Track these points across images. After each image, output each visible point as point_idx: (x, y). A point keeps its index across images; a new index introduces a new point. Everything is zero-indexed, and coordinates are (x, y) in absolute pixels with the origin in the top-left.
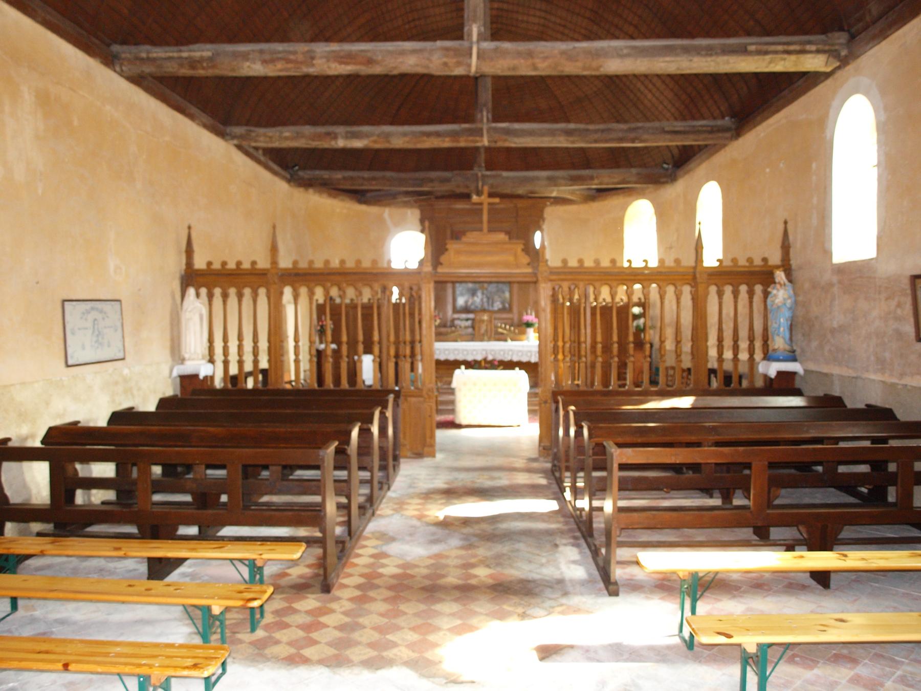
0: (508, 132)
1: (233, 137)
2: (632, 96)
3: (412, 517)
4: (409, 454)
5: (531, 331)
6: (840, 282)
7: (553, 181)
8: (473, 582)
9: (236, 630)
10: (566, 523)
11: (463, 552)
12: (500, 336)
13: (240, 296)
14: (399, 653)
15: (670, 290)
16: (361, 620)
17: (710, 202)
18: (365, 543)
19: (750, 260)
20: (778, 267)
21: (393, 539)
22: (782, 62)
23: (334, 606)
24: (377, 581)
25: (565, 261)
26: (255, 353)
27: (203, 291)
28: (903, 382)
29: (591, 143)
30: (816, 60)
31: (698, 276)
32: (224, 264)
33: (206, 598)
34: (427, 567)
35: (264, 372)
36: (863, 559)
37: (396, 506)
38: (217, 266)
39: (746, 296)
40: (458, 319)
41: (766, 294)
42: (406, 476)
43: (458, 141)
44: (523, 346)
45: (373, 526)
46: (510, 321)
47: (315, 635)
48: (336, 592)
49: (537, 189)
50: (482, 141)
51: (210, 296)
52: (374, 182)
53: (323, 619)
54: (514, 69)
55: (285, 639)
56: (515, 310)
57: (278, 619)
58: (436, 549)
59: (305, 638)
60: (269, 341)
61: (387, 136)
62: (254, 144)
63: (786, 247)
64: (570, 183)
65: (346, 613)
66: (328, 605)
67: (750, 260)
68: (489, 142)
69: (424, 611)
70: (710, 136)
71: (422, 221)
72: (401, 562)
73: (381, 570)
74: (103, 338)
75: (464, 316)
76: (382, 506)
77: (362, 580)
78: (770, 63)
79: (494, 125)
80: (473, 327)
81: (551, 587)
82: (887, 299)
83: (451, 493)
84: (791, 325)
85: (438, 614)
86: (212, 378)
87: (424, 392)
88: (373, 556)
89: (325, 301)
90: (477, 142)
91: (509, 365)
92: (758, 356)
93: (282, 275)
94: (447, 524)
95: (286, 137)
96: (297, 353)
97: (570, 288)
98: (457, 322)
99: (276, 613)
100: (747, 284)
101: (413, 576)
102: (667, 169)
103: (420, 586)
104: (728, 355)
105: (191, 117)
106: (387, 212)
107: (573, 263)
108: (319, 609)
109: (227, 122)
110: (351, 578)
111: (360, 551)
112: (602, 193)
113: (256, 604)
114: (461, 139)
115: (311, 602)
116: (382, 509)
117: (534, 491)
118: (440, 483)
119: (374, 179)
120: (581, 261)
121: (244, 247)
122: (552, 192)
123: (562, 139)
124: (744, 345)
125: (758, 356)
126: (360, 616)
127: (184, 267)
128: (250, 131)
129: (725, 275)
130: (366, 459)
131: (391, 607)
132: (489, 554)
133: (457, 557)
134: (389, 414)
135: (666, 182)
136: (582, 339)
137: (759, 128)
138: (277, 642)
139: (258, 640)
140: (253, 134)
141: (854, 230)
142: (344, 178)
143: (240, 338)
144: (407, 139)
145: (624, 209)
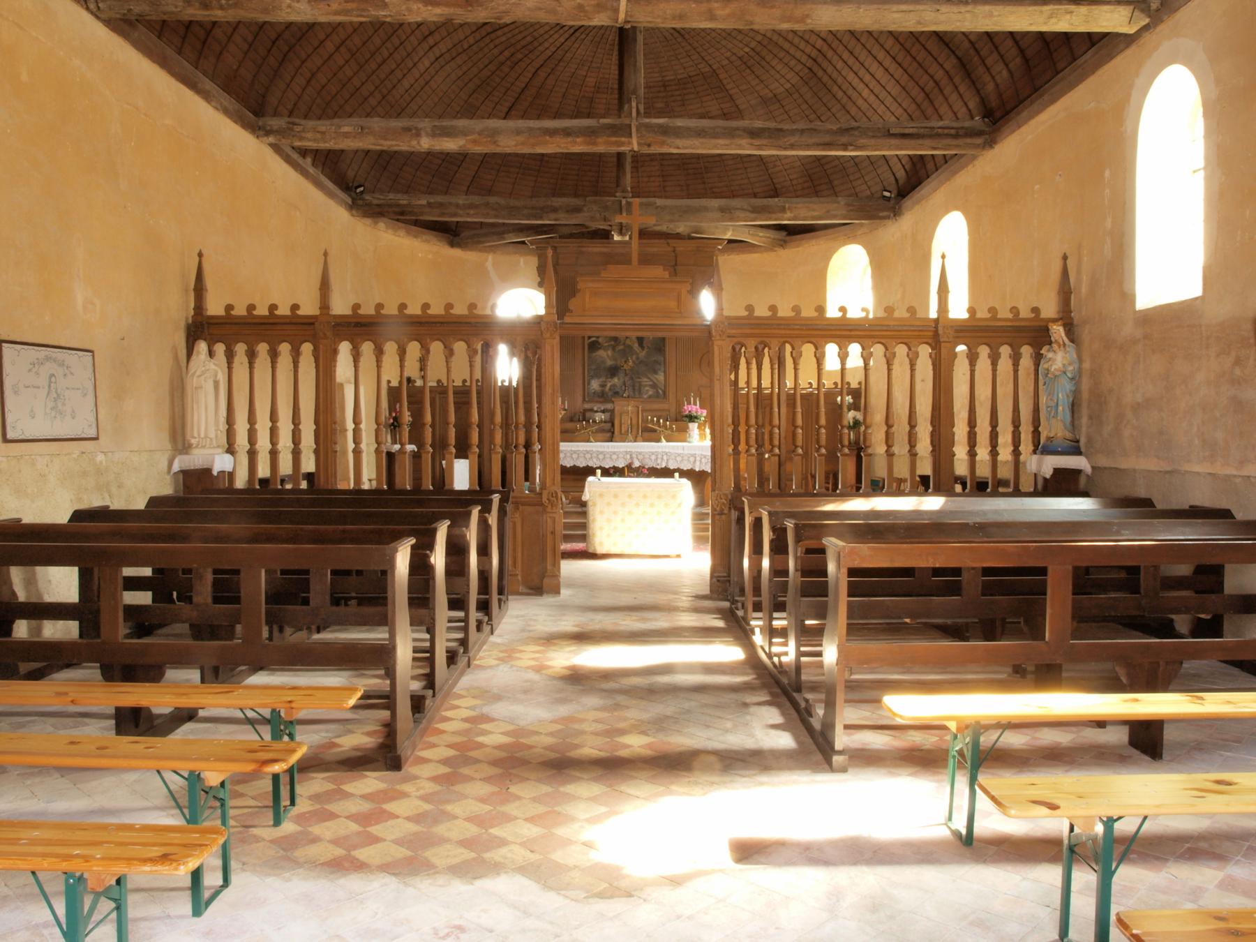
0: (665, 131)
1: (268, 133)
2: (840, 94)
3: (528, 668)
4: (521, 589)
5: (694, 427)
6: (1146, 337)
7: (727, 213)
8: (623, 753)
9: (248, 823)
10: (759, 677)
11: (605, 715)
12: (653, 435)
13: (274, 355)
14: (509, 855)
15: (901, 350)
16: (449, 808)
17: (951, 238)
18: (456, 702)
19: (1014, 310)
20: (1054, 321)
21: (498, 698)
22: (1068, 17)
23: (407, 788)
24: (472, 754)
25: (750, 308)
26: (296, 453)
27: (220, 348)
28: (1245, 473)
29: (785, 149)
30: (1116, 15)
31: (940, 332)
32: (251, 307)
33: (196, 759)
34: (551, 734)
35: (309, 477)
36: (1229, 702)
37: (501, 655)
38: (240, 311)
39: (1010, 362)
41: (1038, 358)
42: (517, 617)
43: (595, 144)
45: (467, 680)
47: (375, 830)
48: (409, 769)
49: (704, 225)
50: (630, 143)
51: (230, 356)
52: (472, 212)
53: (389, 807)
54: (681, 17)
55: (328, 835)
57: (318, 806)
58: (563, 710)
59: (359, 833)
60: (316, 422)
61: (494, 133)
62: (297, 144)
63: (1065, 292)
64: (753, 215)
65: (424, 798)
66: (398, 787)
67: (1014, 310)
68: (639, 144)
69: (547, 794)
70: (954, 142)
71: (541, 270)
72: (511, 728)
73: (480, 739)
74: (64, 404)
76: (481, 654)
77: (451, 753)
78: (1050, 17)
79: (647, 120)
81: (743, 761)
82: (1218, 356)
83: (582, 638)
84: (1073, 405)
85: (572, 798)
86: (231, 475)
87: (545, 499)
88: (466, 720)
89: (400, 382)
90: (623, 144)
91: (666, 473)
92: (1026, 447)
93: (337, 325)
94: (578, 679)
95: (346, 136)
96: (357, 440)
97: (756, 348)
98: (588, 415)
99: (315, 798)
100: (1011, 345)
101: (531, 747)
102: (888, 199)
103: (541, 759)
104: (983, 453)
105: (206, 96)
106: (490, 260)
107: (761, 311)
108: (384, 792)
109: (259, 112)
110: (435, 750)
111: (449, 714)
112: (794, 232)
113: (277, 768)
114: (600, 140)
115: (372, 782)
116: (481, 658)
117: (706, 633)
118: (569, 624)
119: (471, 206)
120: (773, 308)
121: (285, 288)
122: (726, 229)
123: (744, 142)
124: (1005, 439)
125: (1026, 447)
126: (448, 802)
127: (192, 313)
128: (294, 124)
129: (978, 332)
130: (458, 581)
131: (496, 789)
132: (645, 716)
133: (595, 721)
134: (493, 520)
135: (888, 218)
136: (776, 422)
137: (1024, 129)
138: (315, 840)
139: (285, 837)
140: (297, 129)
141: (1168, 262)
142: (430, 205)
143: (274, 417)
144: (520, 138)
145: (827, 259)
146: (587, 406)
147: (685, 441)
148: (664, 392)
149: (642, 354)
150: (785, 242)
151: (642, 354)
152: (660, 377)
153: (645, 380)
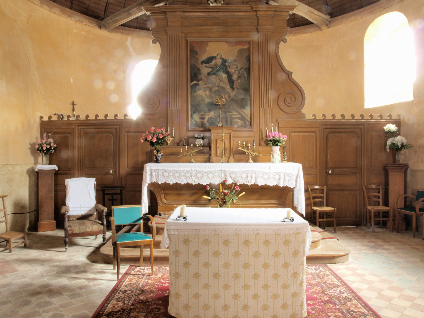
5: (277, 150)
12: (242, 156)
98: (191, 140)
146: (190, 134)
147: (269, 161)
150: (330, 22)
151: (233, 94)
152: (247, 111)
153: (235, 114)
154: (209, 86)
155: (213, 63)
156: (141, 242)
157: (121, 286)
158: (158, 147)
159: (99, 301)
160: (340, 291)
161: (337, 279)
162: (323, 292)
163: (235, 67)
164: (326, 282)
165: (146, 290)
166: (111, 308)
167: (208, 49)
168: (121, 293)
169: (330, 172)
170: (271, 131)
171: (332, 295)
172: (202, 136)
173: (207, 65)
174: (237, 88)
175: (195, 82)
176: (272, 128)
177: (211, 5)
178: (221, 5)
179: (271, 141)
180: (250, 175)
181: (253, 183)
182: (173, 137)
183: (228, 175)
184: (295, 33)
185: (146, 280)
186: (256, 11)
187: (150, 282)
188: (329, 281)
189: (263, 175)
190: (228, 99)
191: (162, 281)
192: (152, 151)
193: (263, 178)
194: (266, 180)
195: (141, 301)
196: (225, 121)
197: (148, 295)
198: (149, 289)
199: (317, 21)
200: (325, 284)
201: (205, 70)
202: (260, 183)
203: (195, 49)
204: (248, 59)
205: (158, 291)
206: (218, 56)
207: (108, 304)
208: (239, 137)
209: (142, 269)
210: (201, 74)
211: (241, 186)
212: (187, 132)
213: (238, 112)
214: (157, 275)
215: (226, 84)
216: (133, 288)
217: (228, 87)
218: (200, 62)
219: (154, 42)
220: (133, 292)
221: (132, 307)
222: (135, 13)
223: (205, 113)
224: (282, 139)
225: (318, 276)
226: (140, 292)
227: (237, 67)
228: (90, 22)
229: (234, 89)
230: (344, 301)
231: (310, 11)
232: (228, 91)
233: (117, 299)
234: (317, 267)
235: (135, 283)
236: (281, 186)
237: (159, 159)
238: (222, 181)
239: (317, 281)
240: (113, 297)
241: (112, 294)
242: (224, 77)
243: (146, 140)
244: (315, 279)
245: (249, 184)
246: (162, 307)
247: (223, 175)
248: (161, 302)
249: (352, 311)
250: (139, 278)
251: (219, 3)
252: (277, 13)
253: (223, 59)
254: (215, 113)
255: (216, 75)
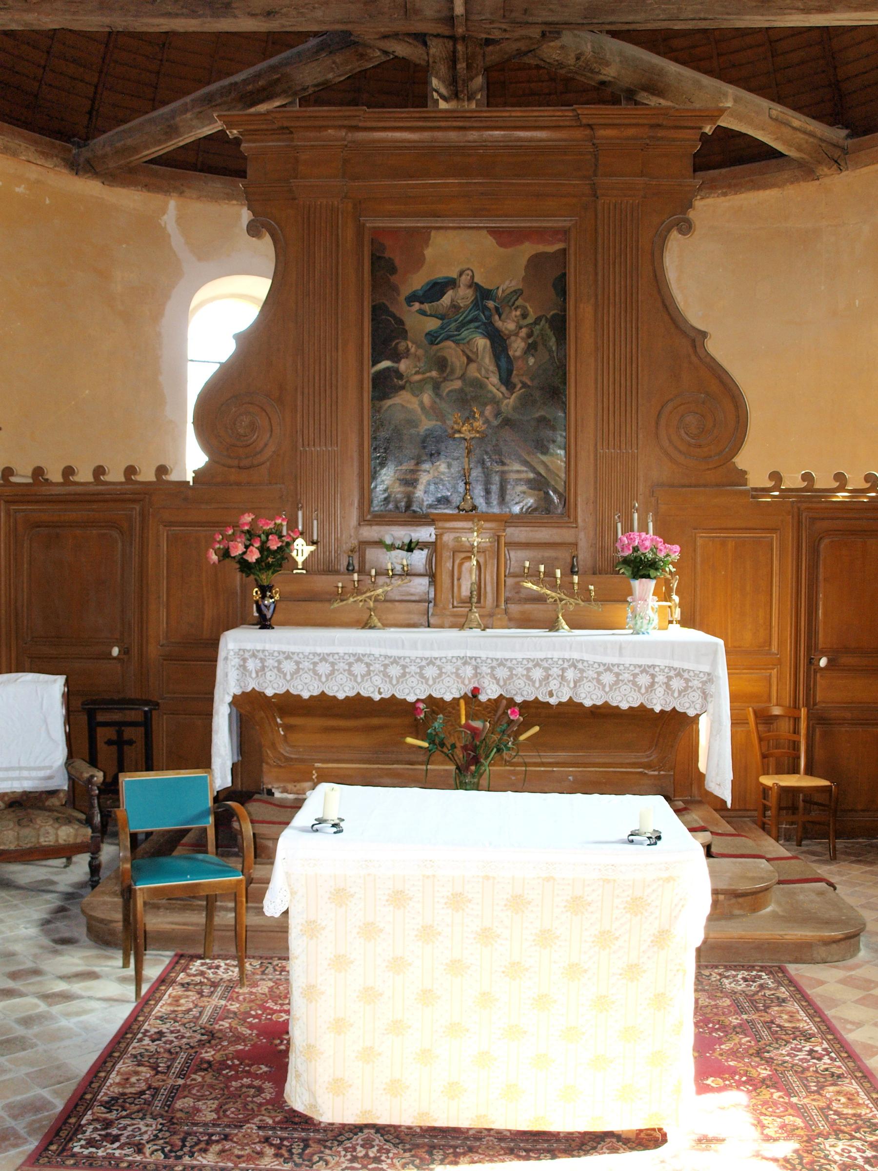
40: (380, 543)
44: (621, 648)
46: (564, 555)
56: (583, 513)
75: (401, 534)
80: (433, 576)
148: (564, 499)
149: (510, 402)
150: (845, 151)
154: (432, 378)
155: (446, 299)
156: (209, 884)
157: (147, 1018)
158: (265, 578)
159: (82, 1063)
160: (811, 1052)
161: (809, 1015)
162: (759, 1053)
163: (518, 313)
164: (772, 1022)
165: (220, 1030)
166: (118, 1084)
167: (429, 252)
168: (147, 1041)
169: (823, 662)
170: (632, 530)
171: (785, 1062)
172: (407, 541)
173: (426, 307)
174: (524, 385)
175: (385, 364)
176: (636, 516)
177: (443, 105)
178: (473, 106)
179: (626, 561)
180: (555, 671)
181: (564, 699)
182: (313, 543)
183: (485, 669)
184: (729, 186)
185: (223, 1002)
186: (590, 126)
187: (234, 1007)
188: (783, 1020)
189: (599, 674)
190: (491, 419)
191: (270, 1004)
192: (246, 590)
193: (598, 681)
194: (607, 689)
195: (205, 1066)
196: (482, 494)
197: (225, 1048)
198: (231, 1028)
199: (799, 149)
200: (770, 1028)
201: (419, 322)
202: (589, 698)
203: (387, 255)
204: (561, 287)
205: (258, 1035)
206: (464, 277)
207: (109, 1073)
208: (527, 545)
209: (210, 968)
210: (405, 338)
211: (525, 705)
212: (359, 525)
213: (525, 463)
214: (255, 985)
215: (487, 370)
216: (184, 1025)
217: (495, 379)
218: (402, 298)
219: (253, 230)
220: (183, 1037)
221: (181, 1082)
222: (192, 128)
223: (417, 464)
224: (661, 555)
225: (751, 1001)
226: (205, 1037)
227: (524, 316)
228: (43, 153)
229: (514, 386)
230: (818, 1082)
231: (776, 120)
232: (494, 397)
233: (135, 1056)
234: (754, 973)
235: (190, 1010)
236: (657, 709)
237: (269, 616)
238: (467, 689)
239: (745, 1017)
240: (124, 1052)
241: (119, 1043)
242: (480, 348)
243: (225, 554)
244: (739, 1009)
245: (553, 701)
246: (267, 1085)
247: (469, 671)
248: (264, 1069)
249: (836, 1113)
250: (200, 993)
251: (470, 99)
252: (661, 133)
253: (477, 287)
254: (449, 466)
255: (457, 343)
